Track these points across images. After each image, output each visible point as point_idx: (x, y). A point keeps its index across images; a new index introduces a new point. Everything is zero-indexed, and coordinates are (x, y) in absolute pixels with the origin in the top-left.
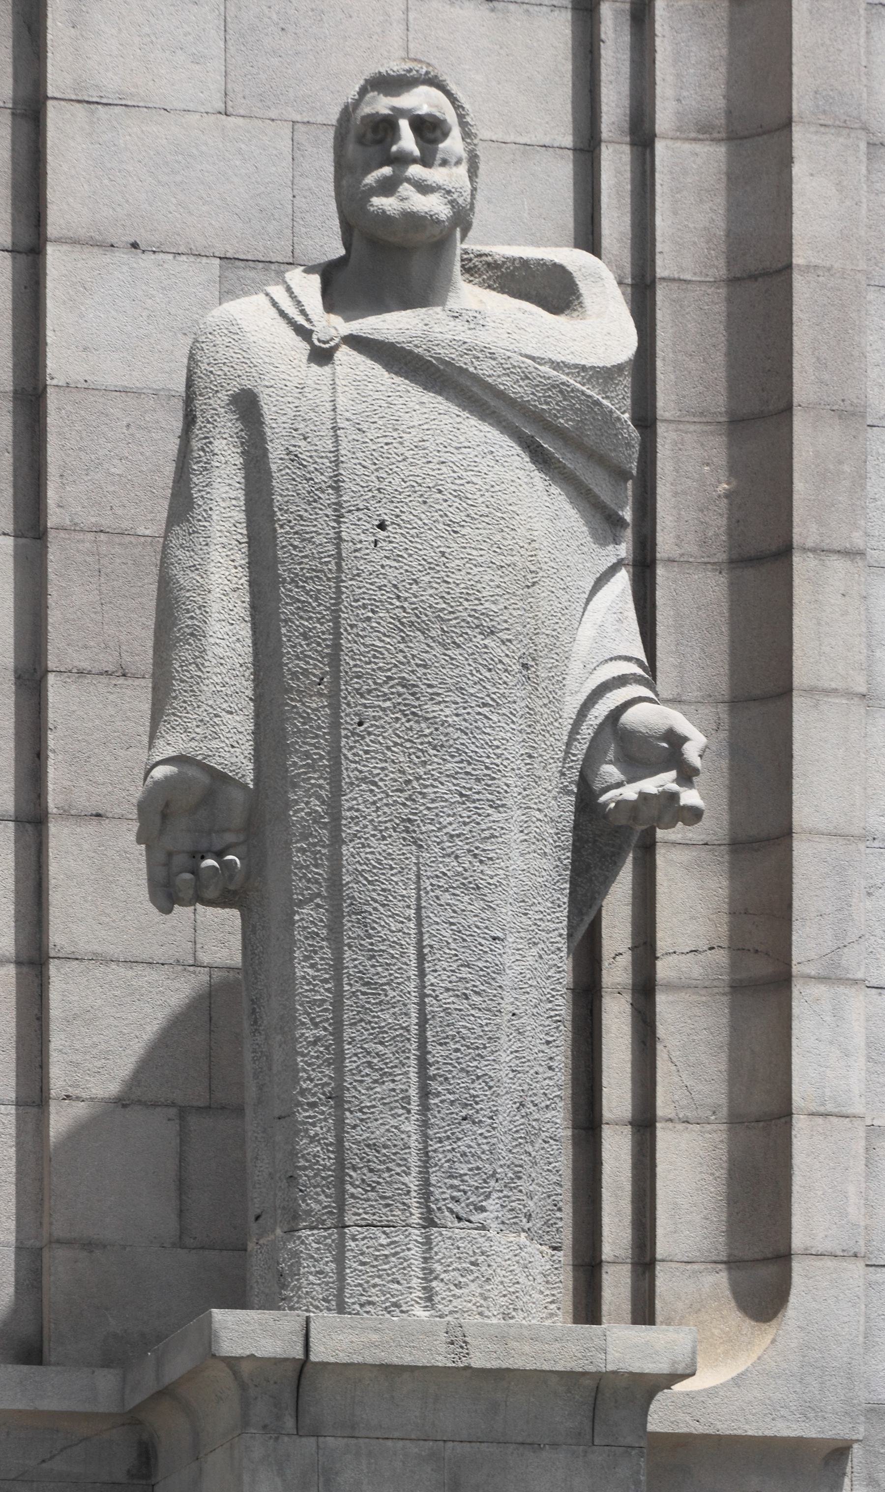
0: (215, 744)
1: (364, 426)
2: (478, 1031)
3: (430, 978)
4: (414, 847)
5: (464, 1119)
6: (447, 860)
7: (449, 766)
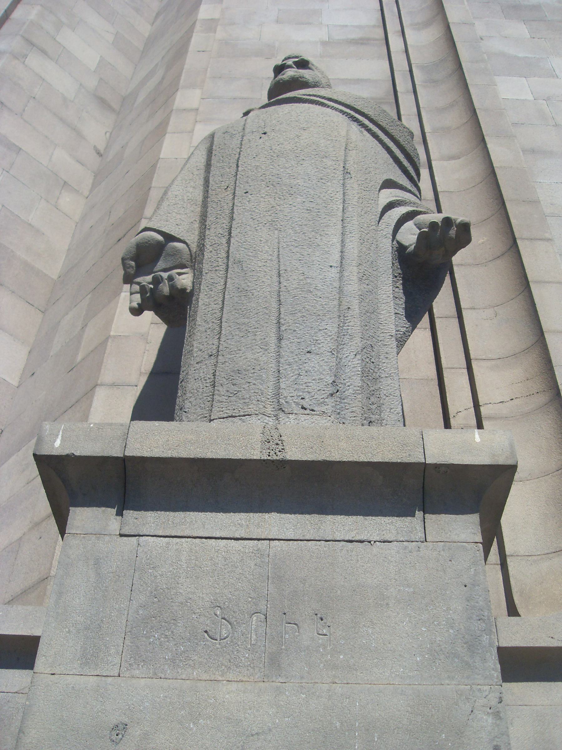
2: (319, 307)
3: (284, 283)
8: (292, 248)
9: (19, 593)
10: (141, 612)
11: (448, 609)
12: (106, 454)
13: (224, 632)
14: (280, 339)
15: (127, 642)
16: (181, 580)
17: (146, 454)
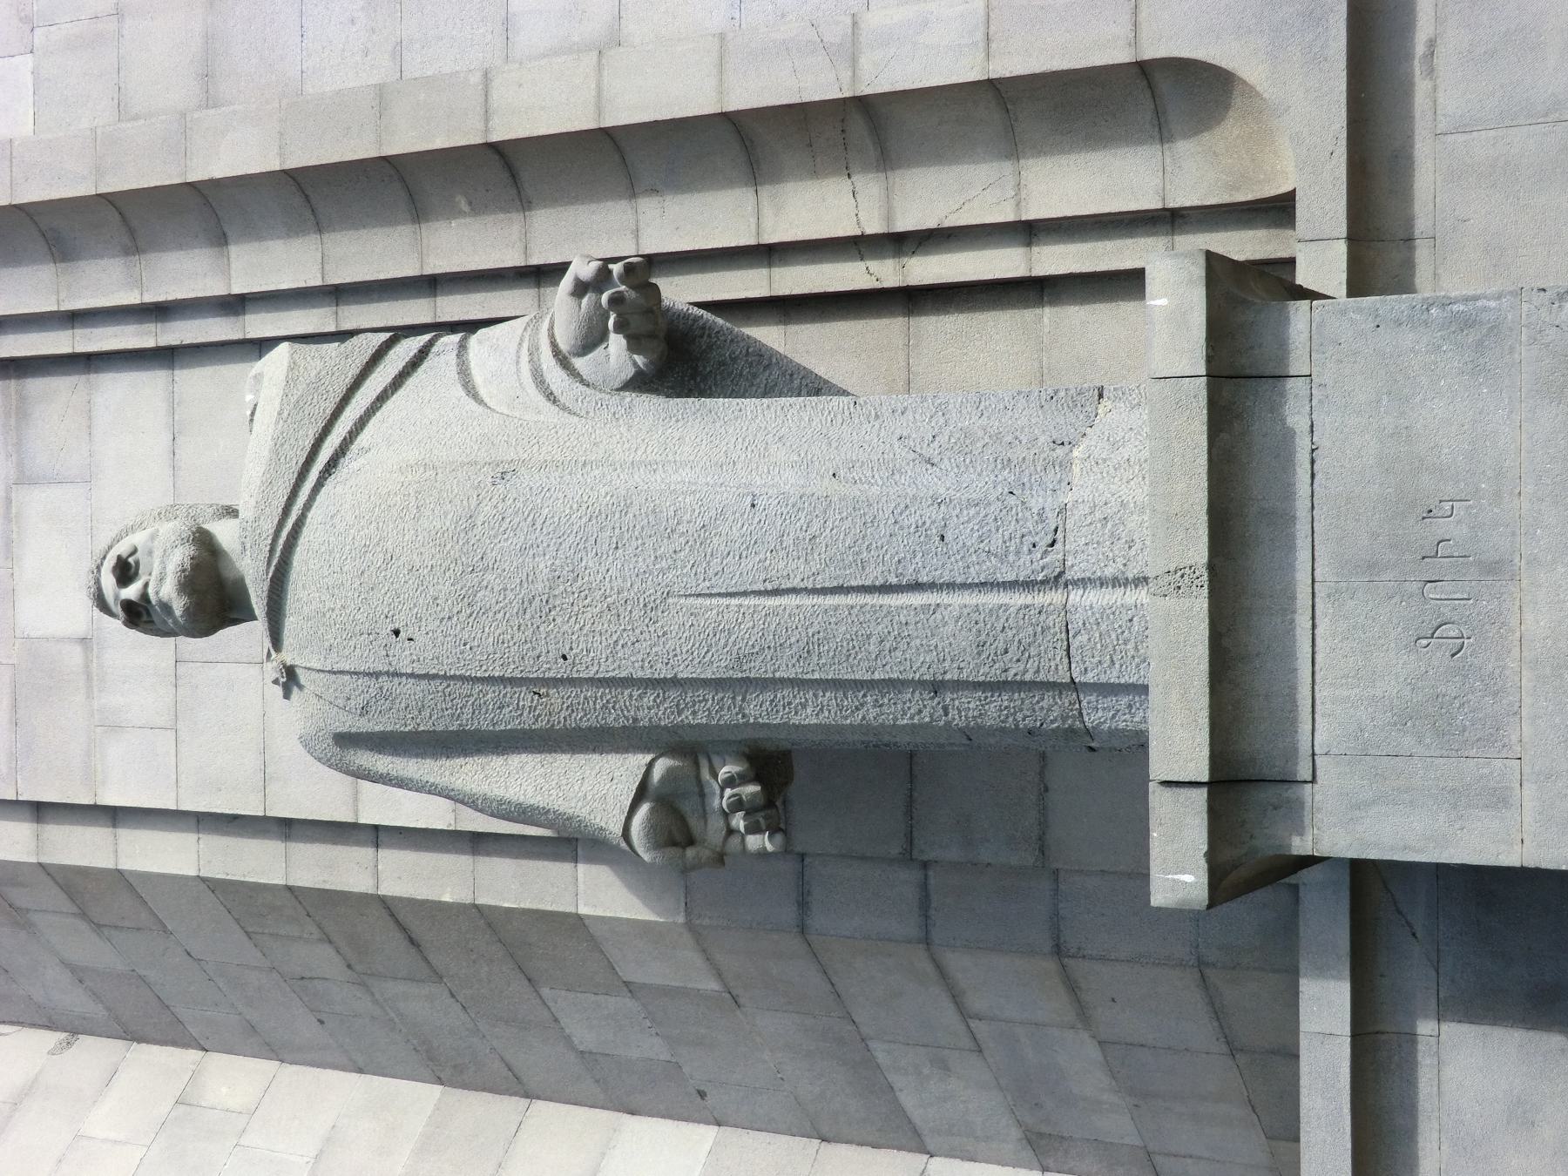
0: (610, 801)
1: (327, 644)
2: (848, 523)
4: (670, 600)
5: (942, 538)
6: (679, 563)
7: (591, 564)
8: (711, 573)
9: (1216, 1024)
10: (1428, 741)
11: (1412, 350)
12: (1205, 808)
13: (1452, 634)
14: (917, 587)
15: (1472, 754)
16: (1379, 693)
17: (1206, 752)
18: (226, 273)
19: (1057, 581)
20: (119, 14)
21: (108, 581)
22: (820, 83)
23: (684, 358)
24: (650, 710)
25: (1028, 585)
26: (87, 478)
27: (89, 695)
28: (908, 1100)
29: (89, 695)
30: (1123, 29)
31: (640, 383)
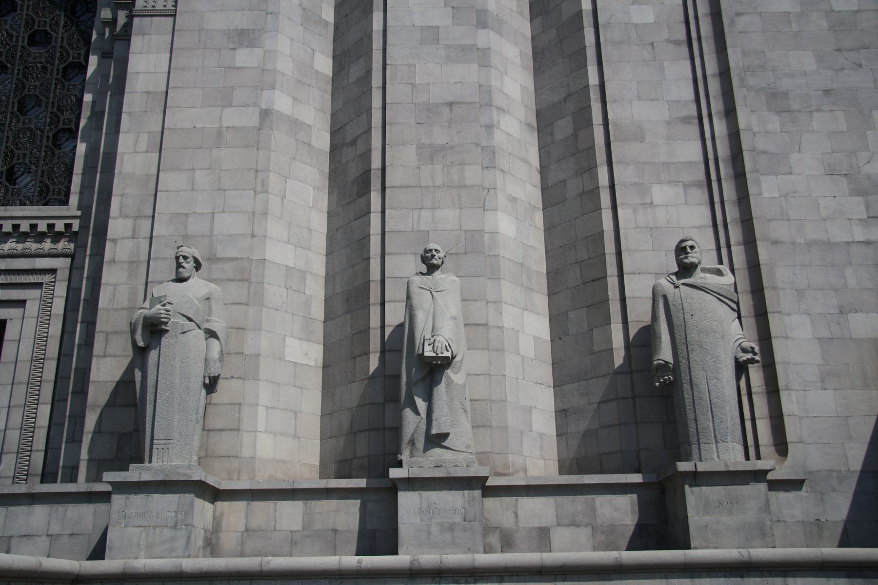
14: (713, 417)
18: (735, 245)
19: (717, 442)
20: (789, 220)
21: (690, 243)
22: (781, 383)
23: (741, 368)
24: (683, 366)
25: (715, 437)
26: (687, 204)
27: (641, 204)
28: (570, 386)
29: (641, 204)
30: (793, 440)
31: (736, 360)
